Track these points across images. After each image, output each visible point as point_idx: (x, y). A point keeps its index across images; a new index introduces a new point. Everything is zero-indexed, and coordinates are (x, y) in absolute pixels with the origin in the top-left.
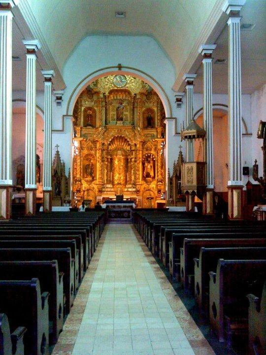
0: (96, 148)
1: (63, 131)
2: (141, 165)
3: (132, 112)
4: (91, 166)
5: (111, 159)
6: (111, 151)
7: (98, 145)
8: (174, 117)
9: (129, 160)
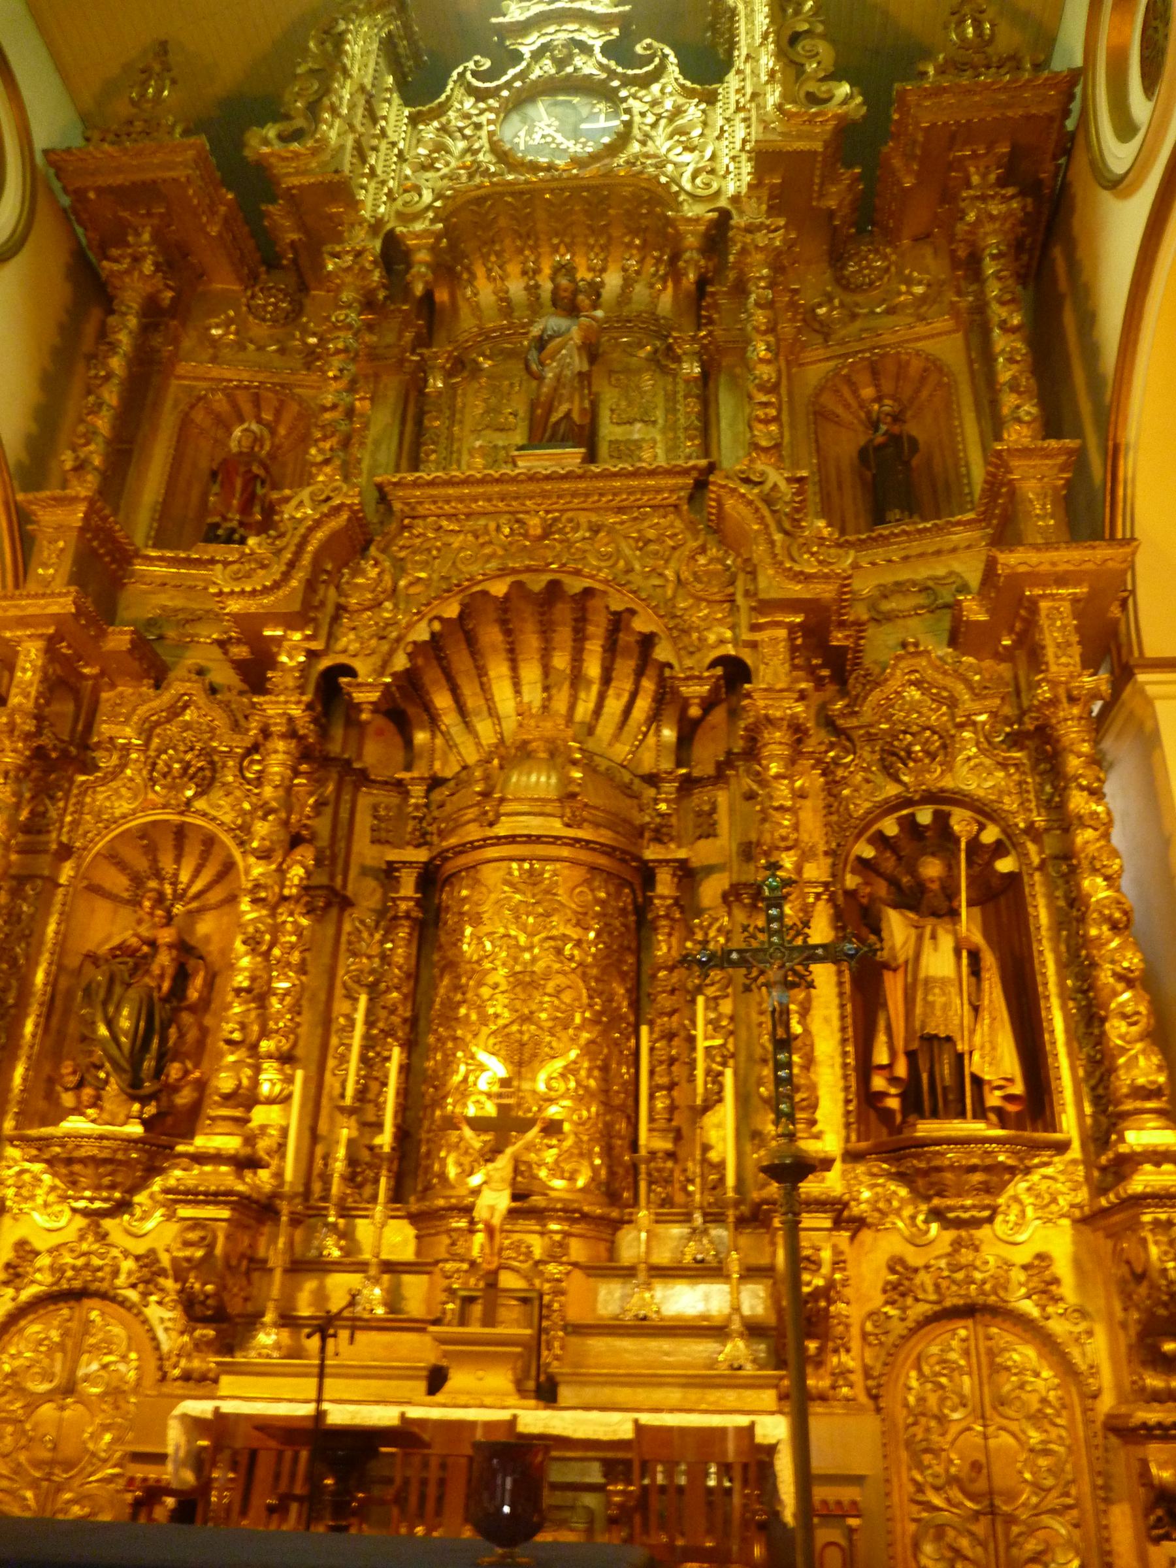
3: (694, 406)
4: (164, 959)
5: (431, 879)
6: (438, 795)
9: (665, 885)
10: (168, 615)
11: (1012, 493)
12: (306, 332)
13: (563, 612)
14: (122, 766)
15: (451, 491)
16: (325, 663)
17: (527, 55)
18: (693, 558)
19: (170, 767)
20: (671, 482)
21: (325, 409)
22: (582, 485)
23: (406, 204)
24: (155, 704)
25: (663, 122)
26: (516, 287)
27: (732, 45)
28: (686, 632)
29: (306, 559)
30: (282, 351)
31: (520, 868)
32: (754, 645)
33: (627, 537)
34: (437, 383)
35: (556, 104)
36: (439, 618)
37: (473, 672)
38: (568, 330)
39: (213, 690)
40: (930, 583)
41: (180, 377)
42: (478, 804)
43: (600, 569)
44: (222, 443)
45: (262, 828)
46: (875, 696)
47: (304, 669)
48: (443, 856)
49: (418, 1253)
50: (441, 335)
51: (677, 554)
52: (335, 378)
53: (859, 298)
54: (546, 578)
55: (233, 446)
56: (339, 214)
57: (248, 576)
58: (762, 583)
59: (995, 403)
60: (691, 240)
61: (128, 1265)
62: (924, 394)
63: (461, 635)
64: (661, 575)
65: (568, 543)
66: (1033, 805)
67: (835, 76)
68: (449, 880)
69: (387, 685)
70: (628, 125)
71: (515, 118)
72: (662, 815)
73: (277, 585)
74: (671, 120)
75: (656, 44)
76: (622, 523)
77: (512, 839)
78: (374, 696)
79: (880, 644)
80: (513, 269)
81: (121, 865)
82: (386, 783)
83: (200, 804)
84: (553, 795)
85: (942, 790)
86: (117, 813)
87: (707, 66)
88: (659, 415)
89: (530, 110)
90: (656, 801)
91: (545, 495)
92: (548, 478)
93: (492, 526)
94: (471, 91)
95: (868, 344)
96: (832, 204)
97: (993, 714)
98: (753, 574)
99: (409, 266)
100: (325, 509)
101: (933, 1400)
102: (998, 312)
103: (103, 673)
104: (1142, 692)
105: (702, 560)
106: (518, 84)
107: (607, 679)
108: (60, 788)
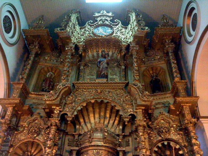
3: (124, 73)
6: (80, 137)
10: (34, 103)
11: (177, 89)
12: (61, 59)
13: (103, 106)
14: (23, 130)
15: (85, 85)
16: (62, 113)
17: (98, 21)
18: (125, 97)
19: (32, 131)
20: (122, 85)
21: (65, 71)
22: (107, 85)
23: (79, 40)
24: (30, 119)
25: (119, 31)
26: (95, 54)
27: (130, 21)
28: (125, 110)
29: (61, 95)
30: (57, 61)
31: (96, 151)
32: (136, 112)
33: (114, 93)
34: (82, 67)
35: (102, 27)
36: (82, 106)
37: (87, 115)
38: (104, 60)
39: (41, 117)
40: (164, 103)
41: (39, 65)
42: (88, 139)
43: (110, 99)
44: (45, 75)
45: (49, 142)
46: (156, 121)
47: (59, 114)
48: (81, 149)
50: (83, 60)
51: (123, 97)
52: (67, 66)
53: (149, 58)
54: (101, 100)
55: (47, 76)
56: (68, 41)
58: (138, 102)
59: (172, 74)
60: (123, 48)
62: (160, 73)
63: (85, 109)
64: (120, 100)
65: (105, 94)
66: (185, 141)
67: (146, 26)
69: (73, 117)
70: (114, 31)
71: (96, 29)
72: (120, 142)
73: (55, 99)
74: (120, 31)
75: (118, 20)
76: (114, 91)
77: (94, 146)
78: (71, 119)
79: (156, 113)
80: (95, 51)
81: (21, 149)
82: (71, 135)
83: (37, 138)
84: (102, 138)
85: (169, 138)
86: (22, 139)
87: (126, 23)
88: (118, 74)
89: (99, 28)
90: (119, 139)
91: (101, 86)
92: (101, 83)
93: (92, 91)
94: (89, 25)
95: (151, 65)
96: (145, 44)
97: (176, 125)
98: (136, 100)
99: (79, 50)
100: (64, 86)
102: (172, 61)
103: (22, 113)
104: (201, 122)
105: (127, 98)
106: (97, 24)
107: (110, 117)
108: (12, 134)
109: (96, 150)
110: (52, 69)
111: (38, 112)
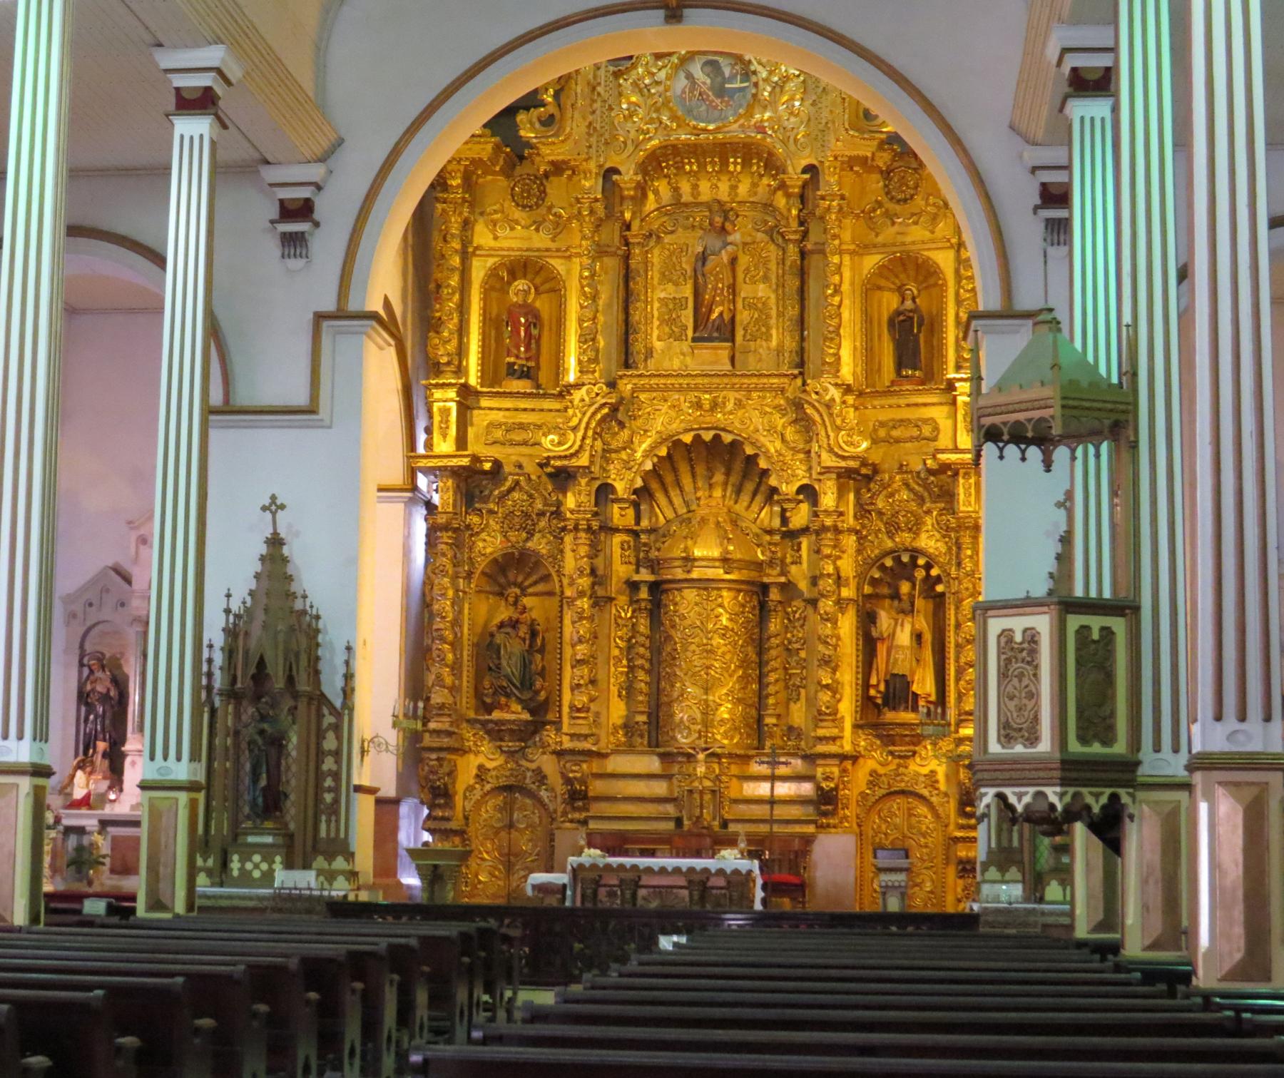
0: (558, 514)
1: (311, 410)
2: (847, 625)
3: (793, 283)
4: (523, 630)
5: (655, 587)
7: (570, 501)
8: (1027, 299)
9: (774, 595)
16: (597, 483)
25: (778, 90)
29: (590, 433)
30: (537, 230)
46: (884, 493)
49: (664, 770)
53: (898, 208)
54: (712, 433)
57: (560, 444)
61: (529, 774)
68: (666, 591)
72: (773, 552)
73: (577, 452)
83: (529, 544)
86: (489, 550)
93: (682, 399)
101: (884, 827)
107: (745, 476)
109: (706, 589)
110: (525, 266)
111: (514, 458)
